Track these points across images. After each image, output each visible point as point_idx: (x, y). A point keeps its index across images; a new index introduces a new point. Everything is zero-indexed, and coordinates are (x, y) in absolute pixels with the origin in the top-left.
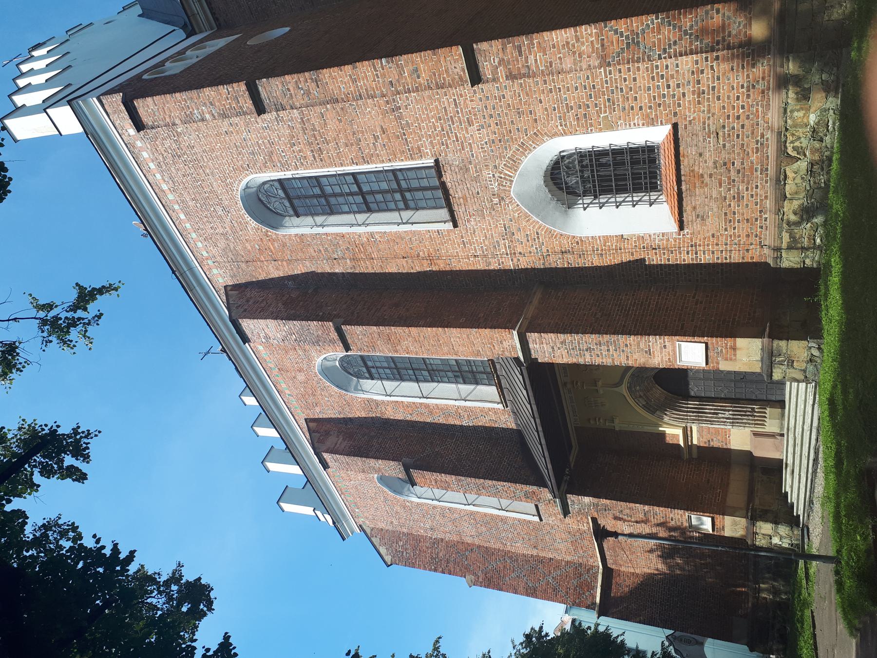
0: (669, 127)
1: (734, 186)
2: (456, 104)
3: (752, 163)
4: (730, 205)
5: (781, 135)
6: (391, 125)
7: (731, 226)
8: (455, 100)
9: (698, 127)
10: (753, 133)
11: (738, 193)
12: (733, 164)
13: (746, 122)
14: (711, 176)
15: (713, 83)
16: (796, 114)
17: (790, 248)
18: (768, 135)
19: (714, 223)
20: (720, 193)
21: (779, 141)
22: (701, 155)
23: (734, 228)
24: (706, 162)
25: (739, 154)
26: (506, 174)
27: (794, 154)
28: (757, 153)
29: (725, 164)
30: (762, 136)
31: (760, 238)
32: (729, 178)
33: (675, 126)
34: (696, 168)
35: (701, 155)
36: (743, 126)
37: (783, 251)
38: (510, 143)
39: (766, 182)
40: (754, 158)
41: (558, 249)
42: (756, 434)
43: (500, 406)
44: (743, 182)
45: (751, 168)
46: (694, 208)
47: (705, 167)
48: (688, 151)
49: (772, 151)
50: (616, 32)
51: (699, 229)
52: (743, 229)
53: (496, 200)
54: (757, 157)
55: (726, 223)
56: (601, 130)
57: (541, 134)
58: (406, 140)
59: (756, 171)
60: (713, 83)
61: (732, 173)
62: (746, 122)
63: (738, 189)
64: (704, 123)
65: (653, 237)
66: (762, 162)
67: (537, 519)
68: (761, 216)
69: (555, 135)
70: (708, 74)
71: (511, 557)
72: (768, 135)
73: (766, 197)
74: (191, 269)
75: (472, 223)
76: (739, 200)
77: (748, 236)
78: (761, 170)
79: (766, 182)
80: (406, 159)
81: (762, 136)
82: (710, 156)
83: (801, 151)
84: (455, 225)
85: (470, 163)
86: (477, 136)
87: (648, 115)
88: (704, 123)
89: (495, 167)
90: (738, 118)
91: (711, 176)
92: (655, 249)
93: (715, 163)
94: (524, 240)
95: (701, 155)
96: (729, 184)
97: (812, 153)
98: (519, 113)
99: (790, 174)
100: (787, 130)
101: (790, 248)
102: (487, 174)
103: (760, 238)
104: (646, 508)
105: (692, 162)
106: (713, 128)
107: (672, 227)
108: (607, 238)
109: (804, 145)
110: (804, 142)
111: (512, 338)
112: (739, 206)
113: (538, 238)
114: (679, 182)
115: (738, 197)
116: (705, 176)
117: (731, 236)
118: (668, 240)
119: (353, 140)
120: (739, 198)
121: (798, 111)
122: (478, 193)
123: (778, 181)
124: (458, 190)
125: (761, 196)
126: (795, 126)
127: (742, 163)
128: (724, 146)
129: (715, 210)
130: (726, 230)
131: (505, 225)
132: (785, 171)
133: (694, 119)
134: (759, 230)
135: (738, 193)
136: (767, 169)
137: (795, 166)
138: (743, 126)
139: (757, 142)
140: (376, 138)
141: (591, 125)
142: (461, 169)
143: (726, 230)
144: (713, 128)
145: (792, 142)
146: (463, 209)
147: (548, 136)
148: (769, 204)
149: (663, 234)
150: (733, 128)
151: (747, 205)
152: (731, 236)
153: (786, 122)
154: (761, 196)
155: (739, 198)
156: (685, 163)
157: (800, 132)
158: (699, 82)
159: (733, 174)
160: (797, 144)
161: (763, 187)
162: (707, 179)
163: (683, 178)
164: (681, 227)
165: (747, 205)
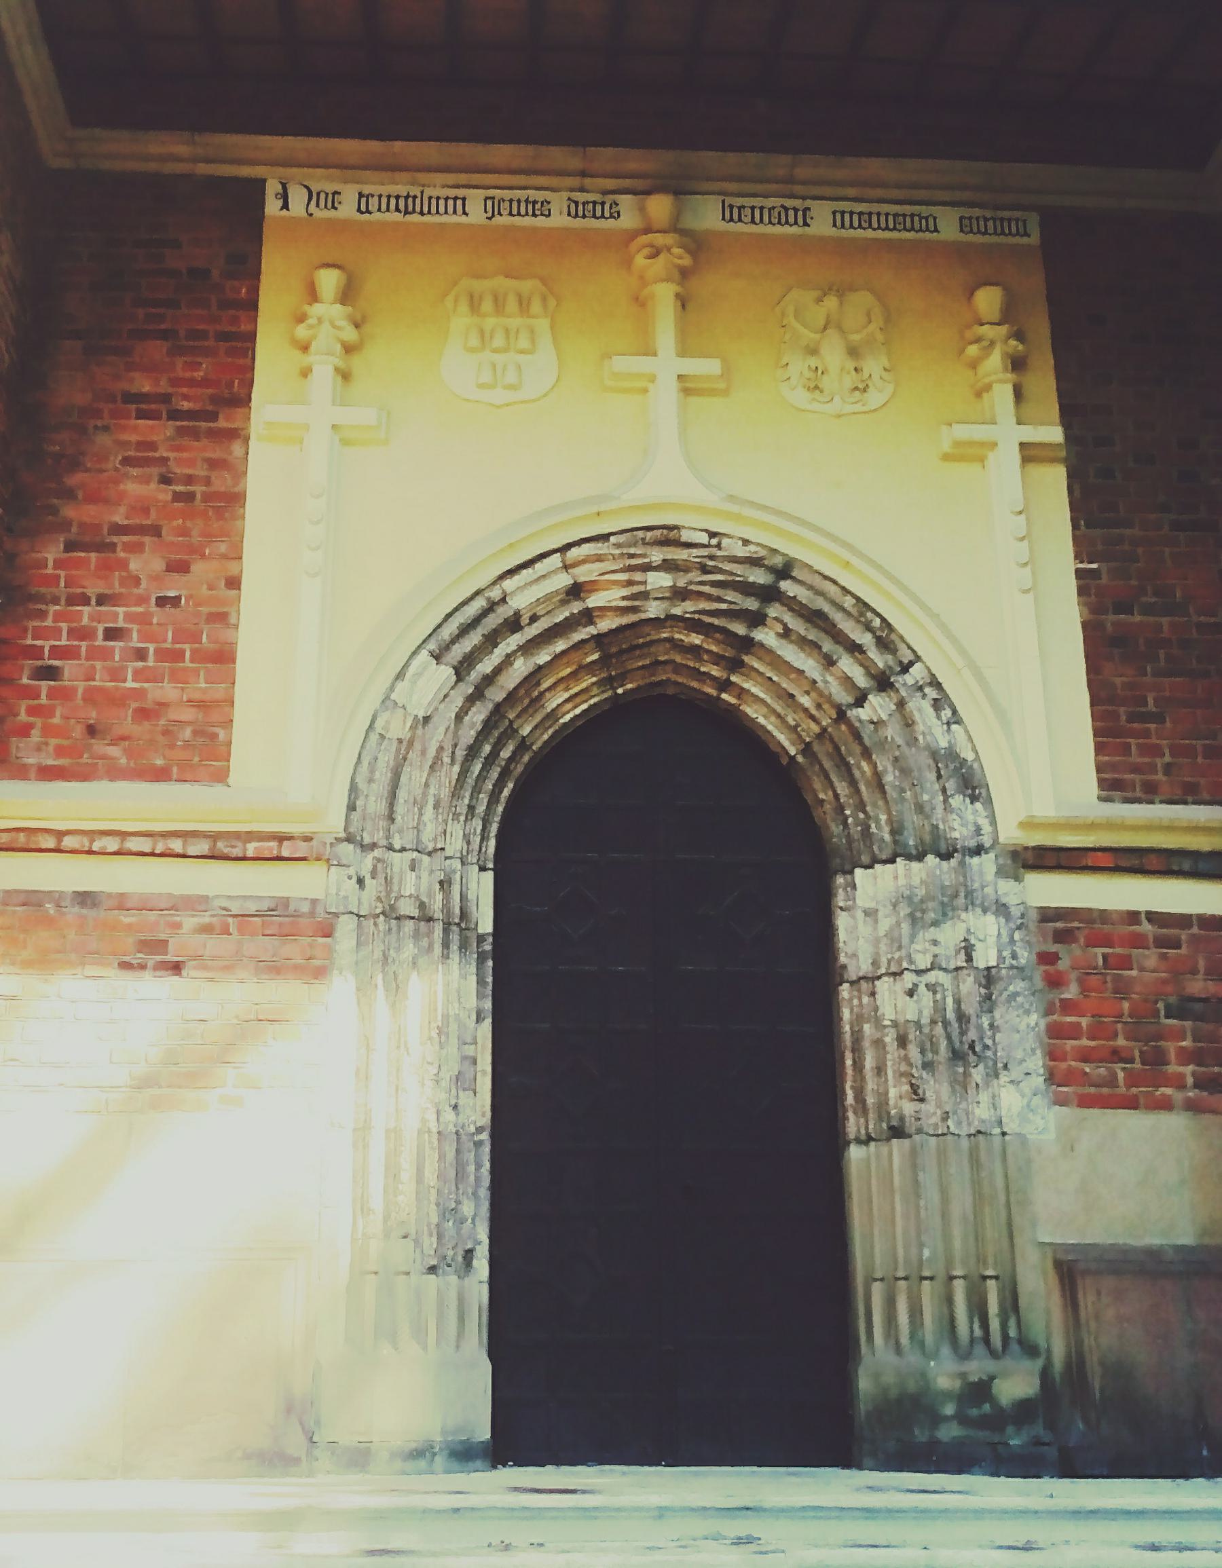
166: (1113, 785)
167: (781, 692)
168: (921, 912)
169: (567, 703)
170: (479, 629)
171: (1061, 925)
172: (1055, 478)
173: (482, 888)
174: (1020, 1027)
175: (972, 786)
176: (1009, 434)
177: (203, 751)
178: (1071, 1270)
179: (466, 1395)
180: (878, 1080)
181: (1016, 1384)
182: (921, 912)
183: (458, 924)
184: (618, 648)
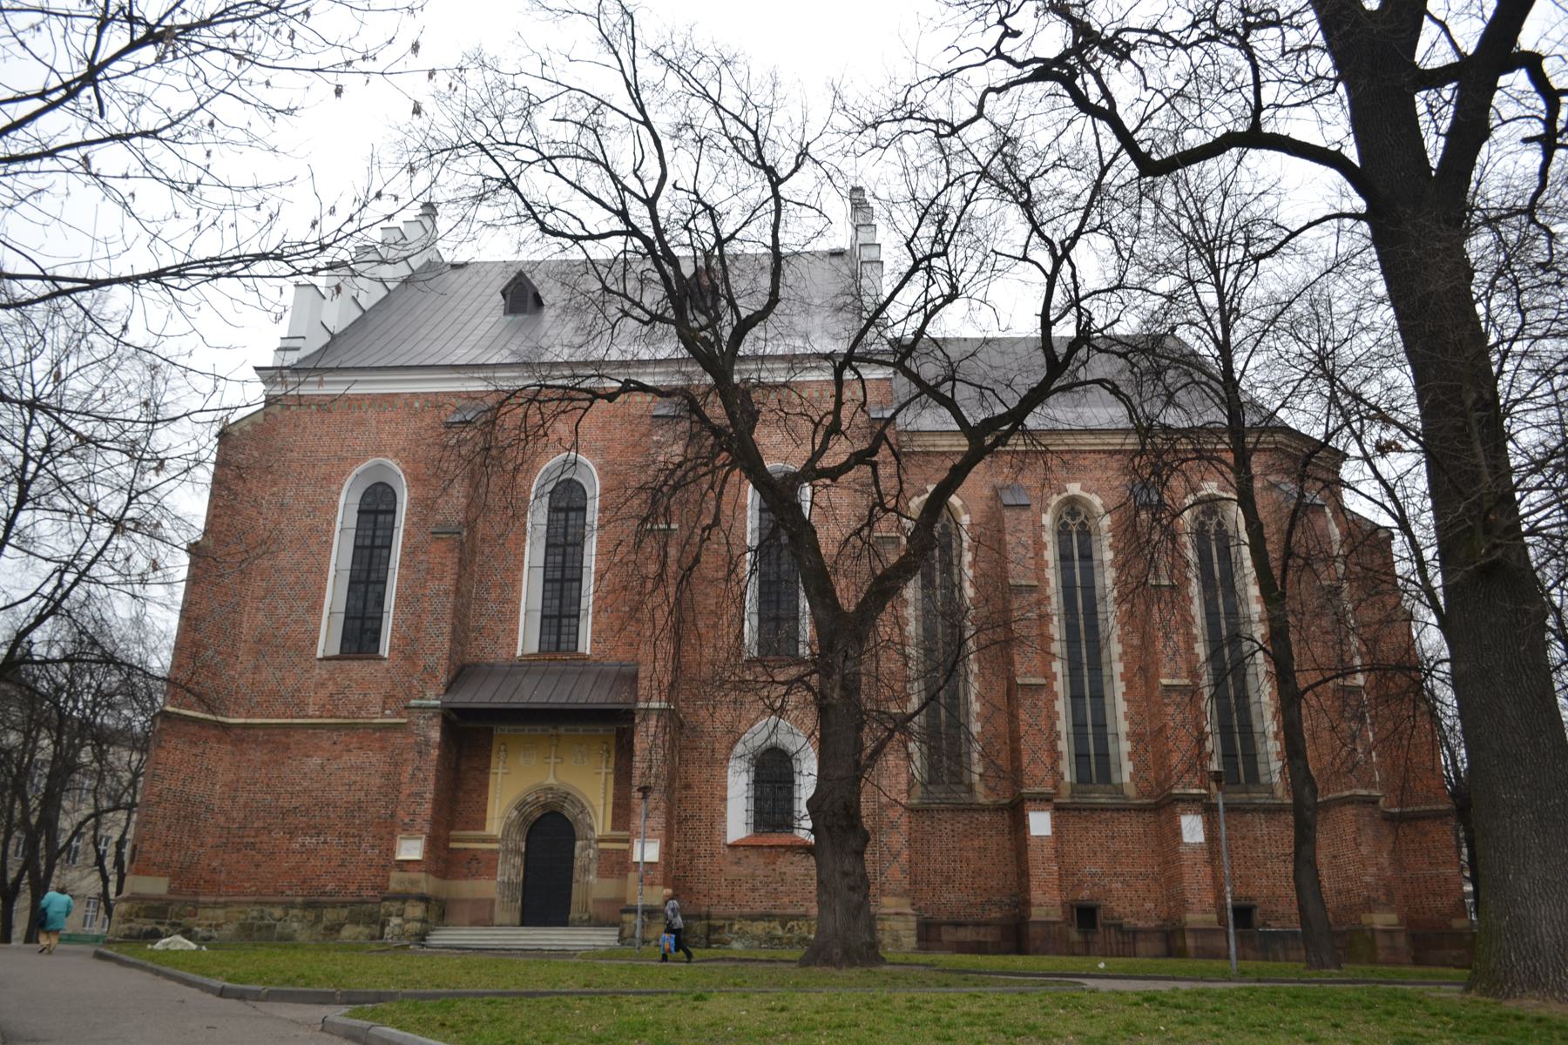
17: (709, 926)
19: (733, 871)
40: (786, 900)
42: (492, 902)
43: (519, 653)
49: (790, 911)
52: (725, 892)
67: (320, 654)
71: (238, 604)
82: (789, 870)
83: (791, 930)
104: (428, 796)
107: (731, 839)
108: (725, 789)
110: (797, 932)
114: (771, 847)
120: (753, 889)
148: (747, 910)
155: (753, 889)
157: (805, 929)
164: (730, 846)
166: (613, 829)
167: (569, 811)
168: (584, 849)
169: (538, 814)
170: (521, 805)
171: (602, 851)
172: (611, 778)
173: (523, 845)
174: (594, 867)
175: (592, 829)
176: (604, 770)
177: (483, 827)
178: (595, 901)
179: (517, 917)
180: (576, 875)
181: (586, 917)
182: (584, 849)
183: (517, 852)
184: (544, 806)
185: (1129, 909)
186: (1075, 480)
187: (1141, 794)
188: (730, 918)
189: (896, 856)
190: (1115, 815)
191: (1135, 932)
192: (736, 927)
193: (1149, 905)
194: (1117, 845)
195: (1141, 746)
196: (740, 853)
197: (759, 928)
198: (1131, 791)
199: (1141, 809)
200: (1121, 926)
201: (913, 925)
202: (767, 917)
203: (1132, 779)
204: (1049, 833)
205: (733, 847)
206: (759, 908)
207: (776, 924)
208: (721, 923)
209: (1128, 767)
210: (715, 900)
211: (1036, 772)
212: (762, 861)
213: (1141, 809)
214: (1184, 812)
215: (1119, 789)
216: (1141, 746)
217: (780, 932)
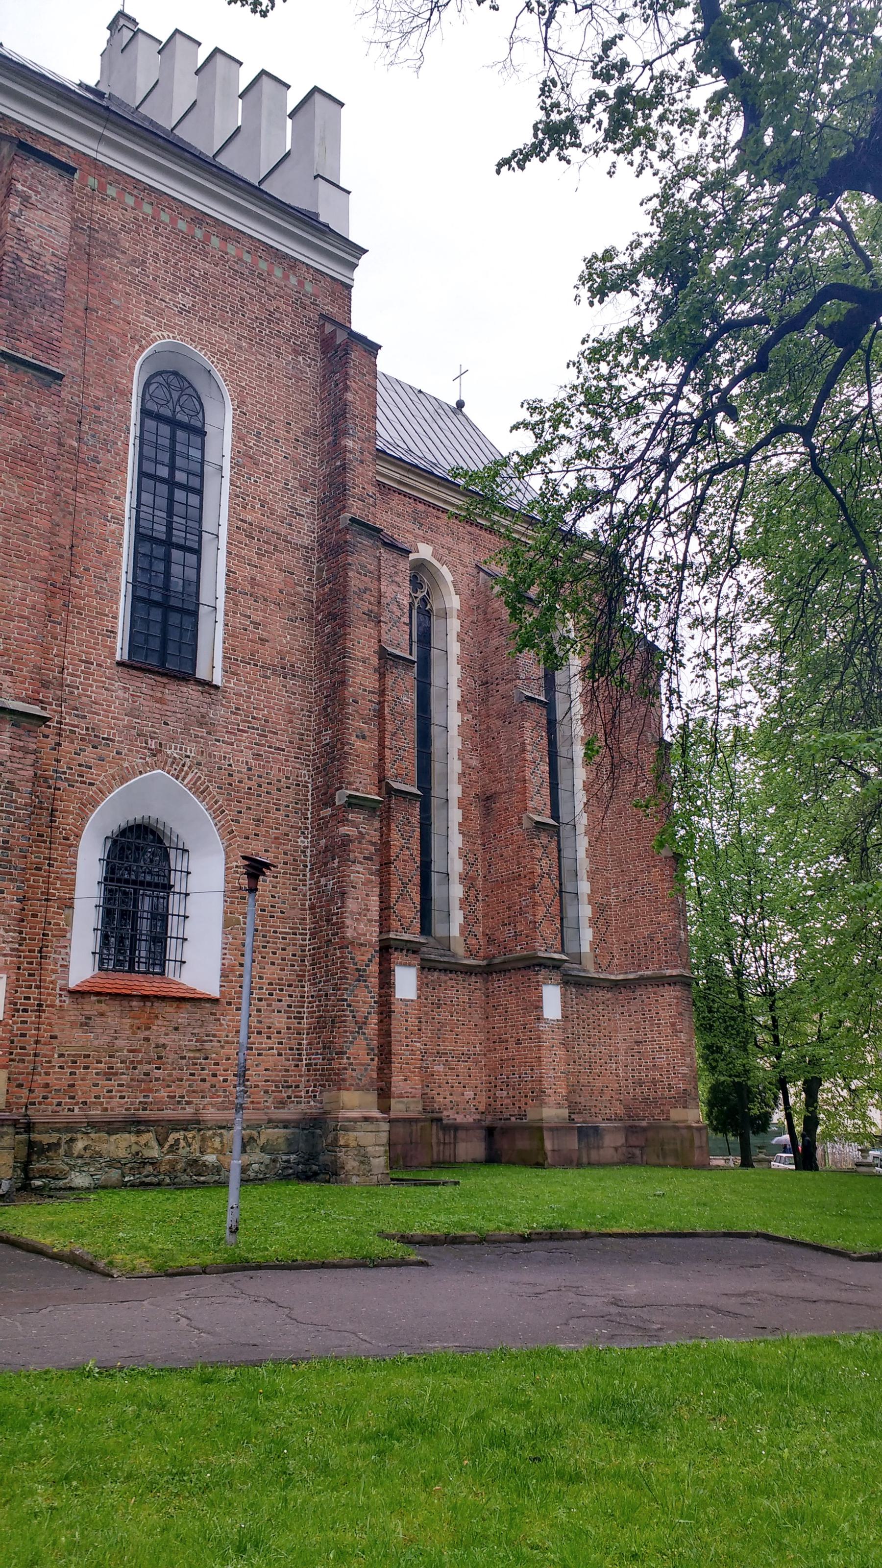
0: (215, 993)
1: (128, 1068)
2: (278, 749)
3: (157, 1091)
4: (100, 1062)
5: (195, 1124)
6: (266, 654)
7: (66, 1062)
8: (283, 750)
9: (211, 1028)
10: (194, 1092)
11: (116, 1074)
12: (159, 1068)
13: (207, 1085)
14: (147, 1039)
15: (257, 1049)
16: (218, 1139)
17: (31, 1144)
18: (189, 1110)
19: (75, 1039)
20: (121, 1050)
21: (189, 1122)
22: (176, 1029)
23: (61, 1067)
24: (166, 1034)
25: (170, 1075)
26: (187, 774)
27: (171, 1139)
28: (168, 1097)
29: (160, 1058)
30: (188, 1103)
31: (40, 1103)
32: (140, 1062)
33: (215, 1001)
34: (160, 1023)
35: (176, 1029)
36: (204, 1080)
37: (24, 1136)
38: (227, 797)
39: (126, 1110)
41: (60, 805)
44: (132, 1080)
45: (151, 1091)
46: (102, 1015)
47: (159, 1032)
48: (182, 1016)
49: (168, 1113)
50: (370, 961)
51: (67, 1018)
52: (58, 1079)
53: (153, 744)
54: (163, 1097)
55: (73, 1056)
56: (225, 913)
57: (230, 839)
58: (249, 664)
59: (144, 1097)
60: (257, 1049)
61: (146, 1067)
62: (207, 1085)
63: (123, 1074)
64: (214, 1036)
65: (63, 950)
66: (156, 1103)
68: (77, 1104)
69: (227, 856)
70: (266, 1043)
72: (189, 1110)
73: (106, 1109)
74: (101, 138)
75: (120, 693)
76: (106, 1074)
77: (47, 1085)
78: (146, 1103)
79: (126, 1110)
80: (225, 650)
81: (188, 1103)
82: (171, 1040)
84: (119, 664)
85: (209, 733)
86: (239, 756)
87: (232, 971)
88: (214, 1036)
89: (199, 764)
90: (214, 1075)
91: (147, 1039)
92: (40, 952)
93: (164, 1046)
94: (82, 759)
95: (171, 1033)
96: (132, 1062)
97: (170, 1161)
98: (258, 820)
99: (145, 1138)
100: (200, 1130)
101: (31, 1144)
102: (192, 750)
103: (40, 1103)
105: (169, 1017)
106: (207, 1045)
109: (181, 1151)
111: (18, 698)
112: (97, 1074)
113: (82, 782)
114: (145, 998)
115: (112, 1074)
116: (147, 1033)
117: (49, 1062)
118: (54, 972)
119: (259, 592)
120: (110, 1074)
121: (221, 1142)
122: (166, 724)
123: (139, 1123)
124: (173, 697)
125: (108, 1103)
126: (203, 1139)
127: (157, 1079)
128: (184, 1058)
129: (96, 1043)
130: (61, 1055)
131: (112, 741)
132: (149, 1131)
133: (221, 1025)
134: (55, 1101)
135: (116, 1074)
136: (145, 1109)
137: (154, 1143)
138: (204, 1080)
139: (183, 1097)
140: (257, 625)
141: (232, 903)
142: (203, 717)
143: (61, 1055)
144: (207, 1045)
145: (185, 1138)
146: (145, 690)
147: (228, 846)
149: (66, 966)
150: (203, 1069)
151: (97, 1085)
152: (49, 1062)
153: (209, 1129)
154: (108, 1103)
155: (110, 1074)
156: (169, 1009)
157: (196, 1146)
158: (259, 1033)
159: (146, 1067)
160: (182, 1143)
161: (121, 1106)
162: (142, 1035)
163: (149, 1004)
164: (72, 993)
165: (97, 1085)
185: (449, 1098)
186: (427, 541)
187: (471, 953)
188: (70, 1128)
189: (361, 1025)
190: (443, 977)
191: (456, 1128)
192: (80, 1145)
193: (469, 1094)
194: (443, 1015)
195: (472, 893)
196: (91, 1006)
197: (120, 1145)
198: (459, 948)
199: (469, 971)
200: (440, 1120)
201: (384, 1137)
202: (135, 1124)
203: (462, 933)
204: (413, 996)
205: (78, 994)
206: (118, 1108)
207: (149, 1137)
208: (53, 1138)
209: (457, 917)
210: (39, 1093)
211: (405, 913)
212: (127, 1021)
213: (469, 971)
214: (547, 980)
215: (445, 943)
216: (472, 893)
217: (154, 1152)
